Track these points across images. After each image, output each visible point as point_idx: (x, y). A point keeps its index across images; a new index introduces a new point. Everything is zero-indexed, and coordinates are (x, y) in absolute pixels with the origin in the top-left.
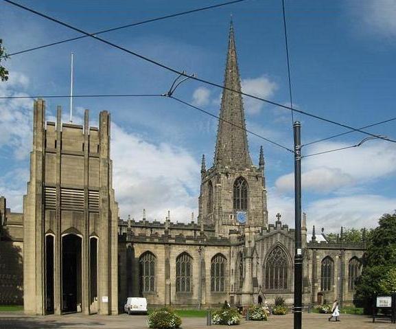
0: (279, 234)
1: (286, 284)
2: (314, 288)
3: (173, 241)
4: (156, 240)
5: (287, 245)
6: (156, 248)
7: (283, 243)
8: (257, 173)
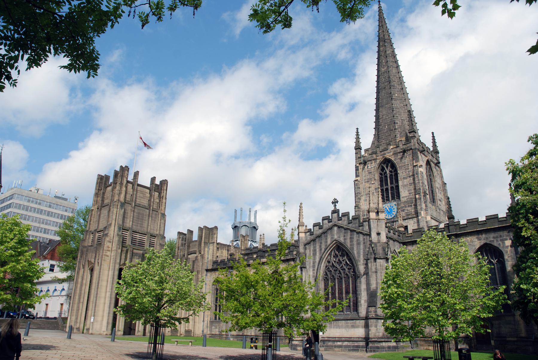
0: (336, 228)
7: (342, 240)
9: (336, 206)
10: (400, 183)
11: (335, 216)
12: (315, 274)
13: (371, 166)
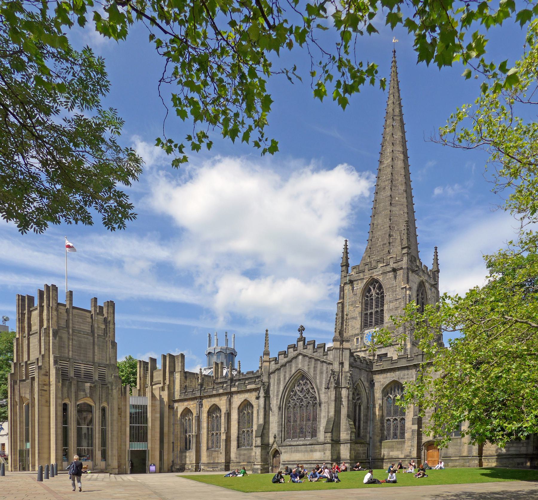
7: (306, 369)
9: (302, 333)
10: (386, 307)
12: (279, 402)
13: (357, 287)
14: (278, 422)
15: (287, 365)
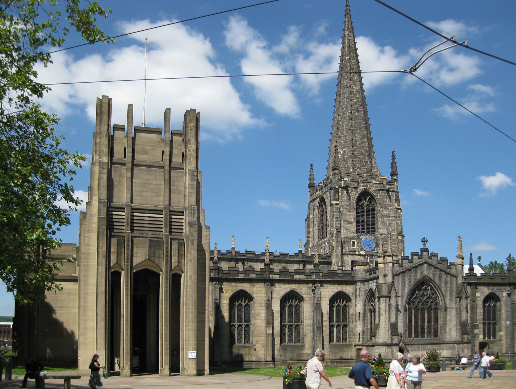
1: (436, 332)
2: (475, 336)
3: (276, 277)
4: (253, 276)
5: (437, 280)
6: (253, 286)
7: (431, 276)
8: (388, 186)
11: (425, 254)
14: (404, 322)
15: (412, 270)
